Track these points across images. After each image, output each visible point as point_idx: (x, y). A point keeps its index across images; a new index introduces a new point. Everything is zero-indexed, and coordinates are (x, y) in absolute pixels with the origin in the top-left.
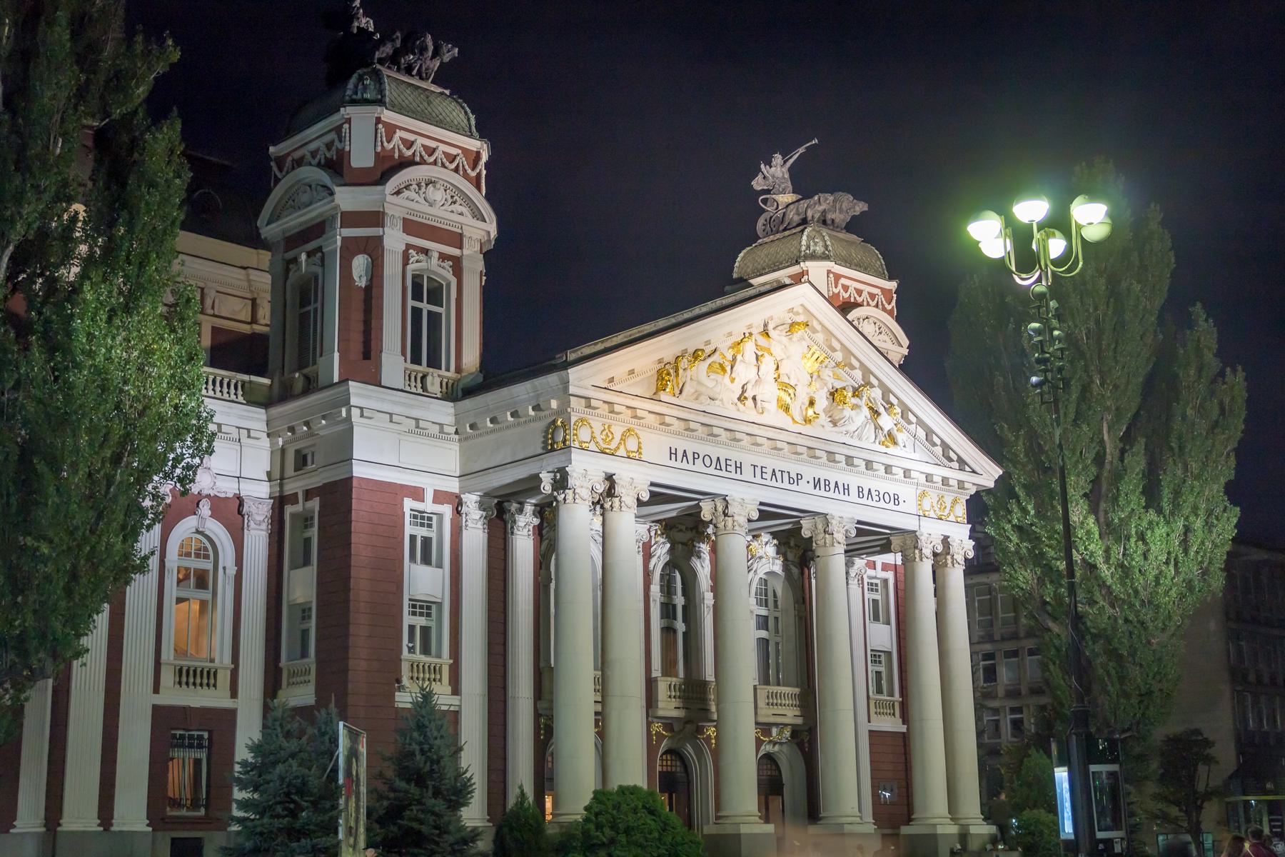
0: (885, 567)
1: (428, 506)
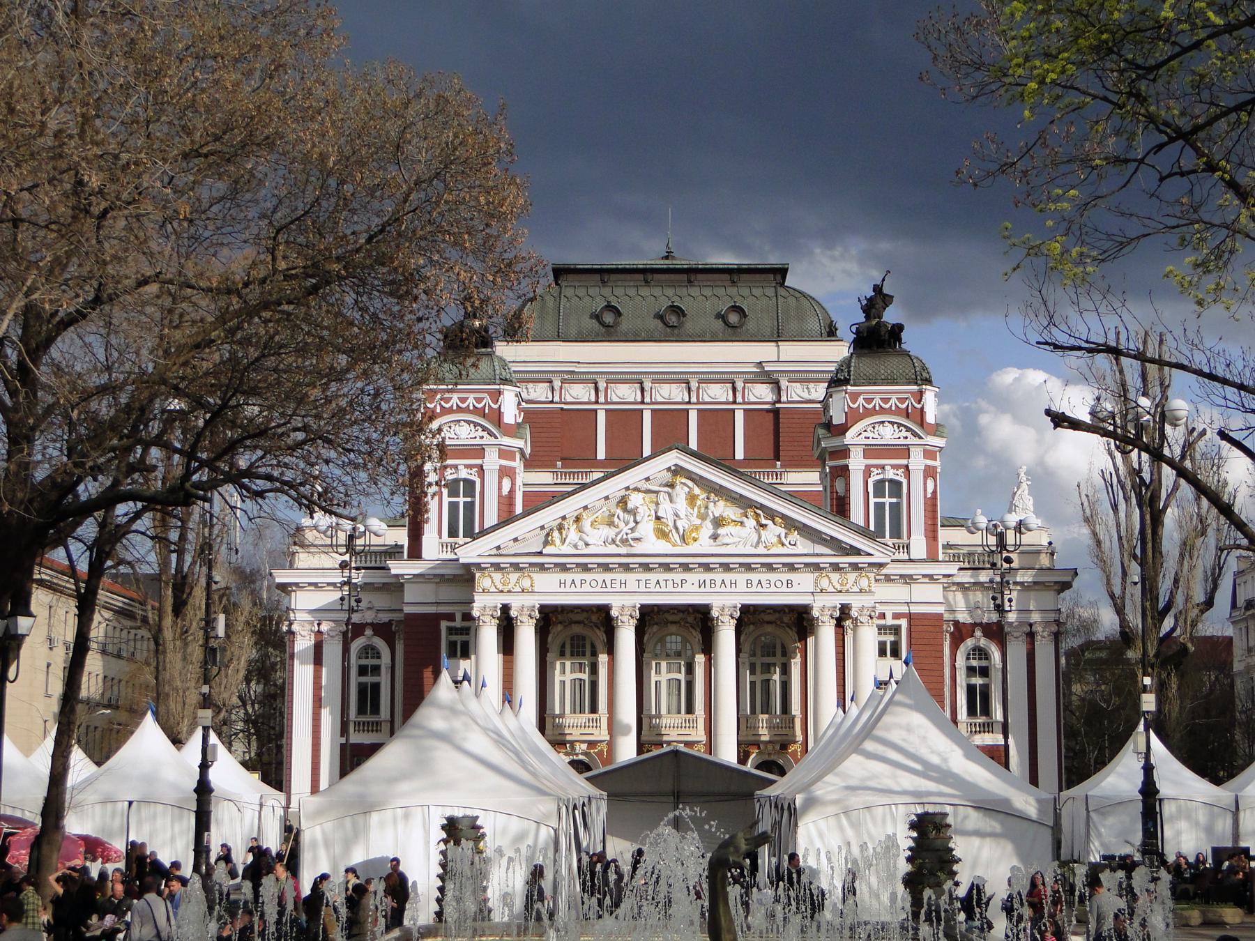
1: (458, 623)
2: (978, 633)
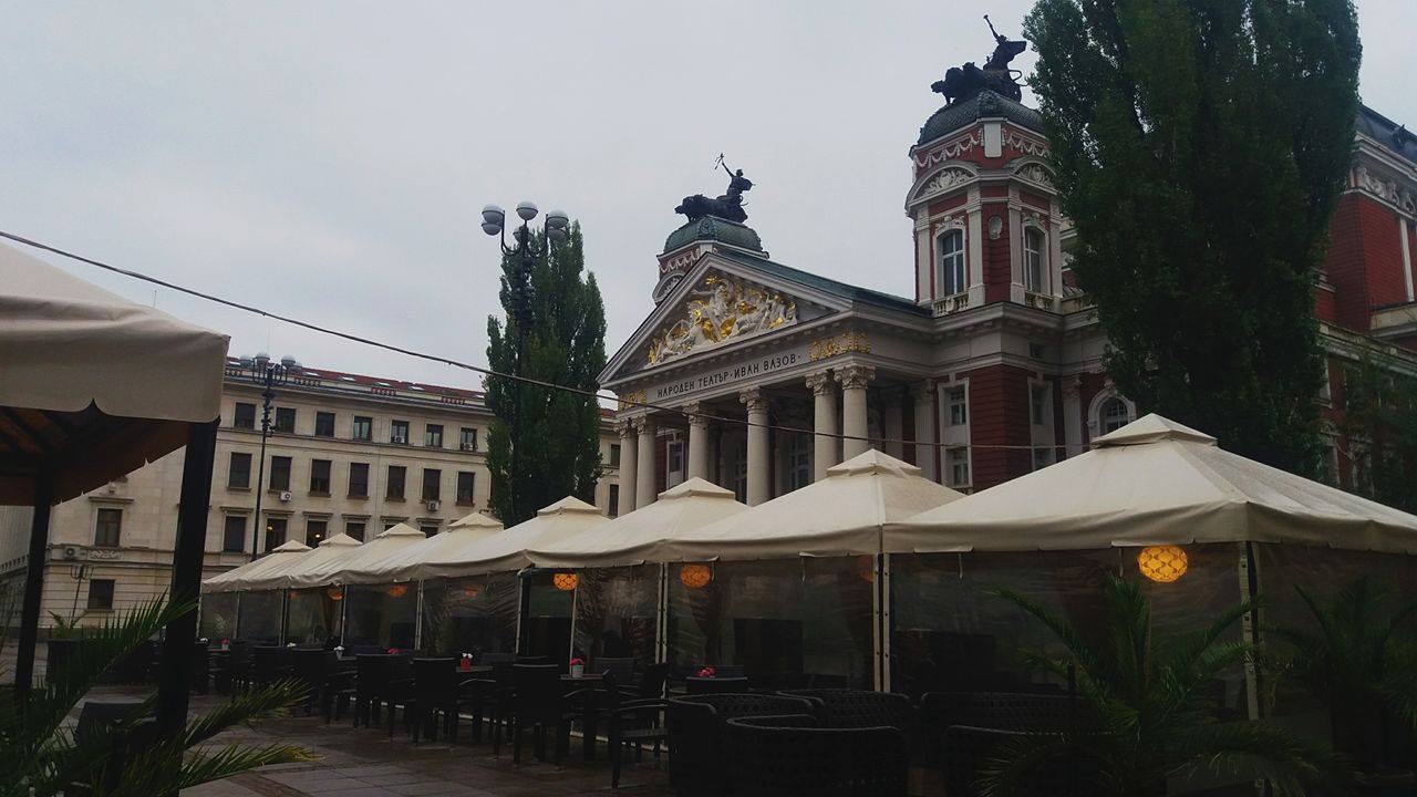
0: (960, 376)
2: (1109, 383)
